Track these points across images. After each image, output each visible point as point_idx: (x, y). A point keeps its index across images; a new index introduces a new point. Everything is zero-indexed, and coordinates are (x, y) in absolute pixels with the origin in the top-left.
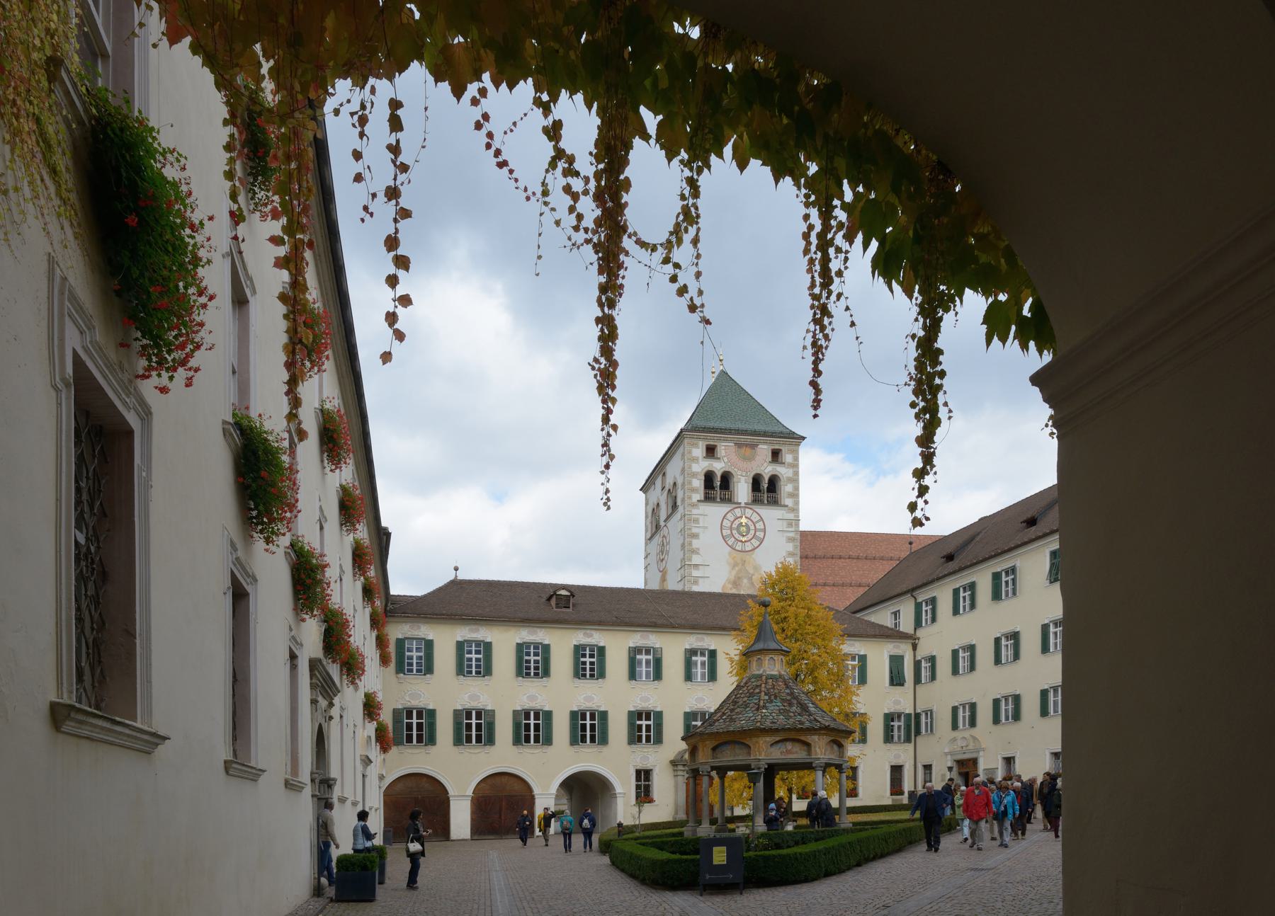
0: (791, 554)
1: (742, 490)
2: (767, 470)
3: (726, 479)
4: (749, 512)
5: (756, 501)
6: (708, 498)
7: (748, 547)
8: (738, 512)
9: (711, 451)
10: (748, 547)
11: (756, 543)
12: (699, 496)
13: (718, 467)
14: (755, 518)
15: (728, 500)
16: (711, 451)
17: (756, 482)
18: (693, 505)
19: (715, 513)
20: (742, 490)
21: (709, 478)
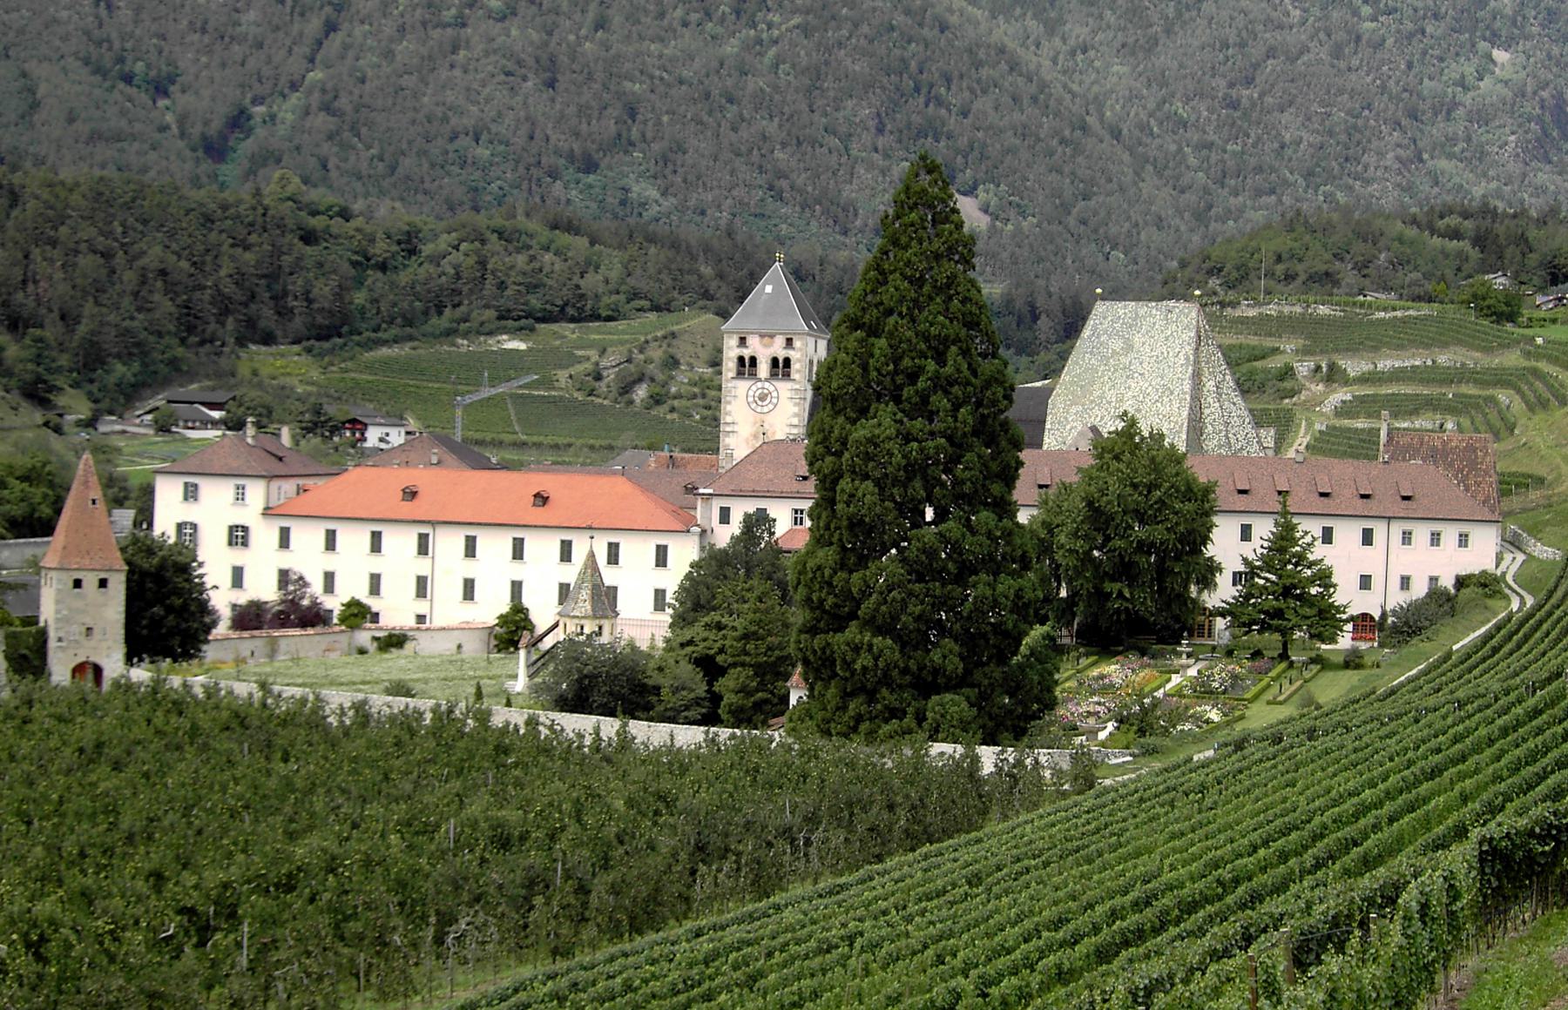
0: (796, 415)
1: (763, 369)
2: (781, 354)
3: (753, 360)
4: (767, 385)
5: (773, 375)
6: (740, 374)
7: (766, 410)
8: (759, 385)
9: (743, 341)
10: (766, 410)
11: (771, 407)
12: (732, 374)
13: (746, 353)
14: (771, 388)
15: (753, 375)
16: (743, 341)
17: (775, 361)
18: (727, 381)
19: (743, 386)
20: (763, 369)
21: (741, 359)
